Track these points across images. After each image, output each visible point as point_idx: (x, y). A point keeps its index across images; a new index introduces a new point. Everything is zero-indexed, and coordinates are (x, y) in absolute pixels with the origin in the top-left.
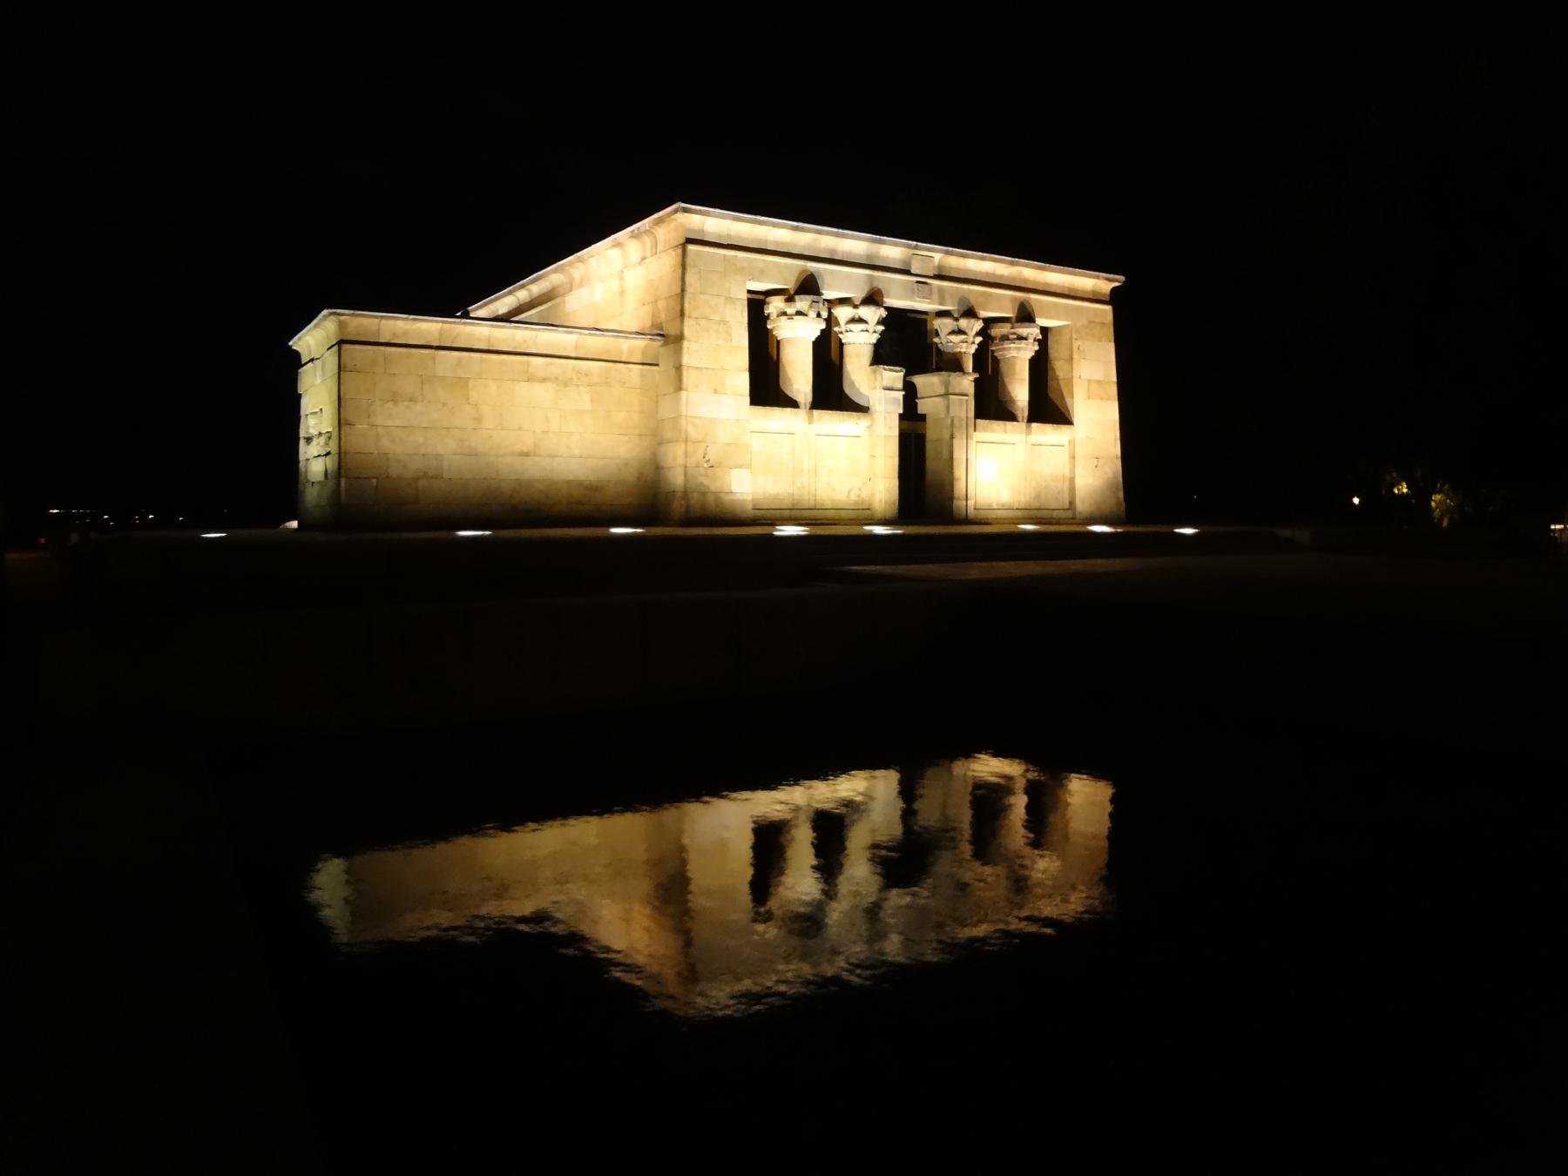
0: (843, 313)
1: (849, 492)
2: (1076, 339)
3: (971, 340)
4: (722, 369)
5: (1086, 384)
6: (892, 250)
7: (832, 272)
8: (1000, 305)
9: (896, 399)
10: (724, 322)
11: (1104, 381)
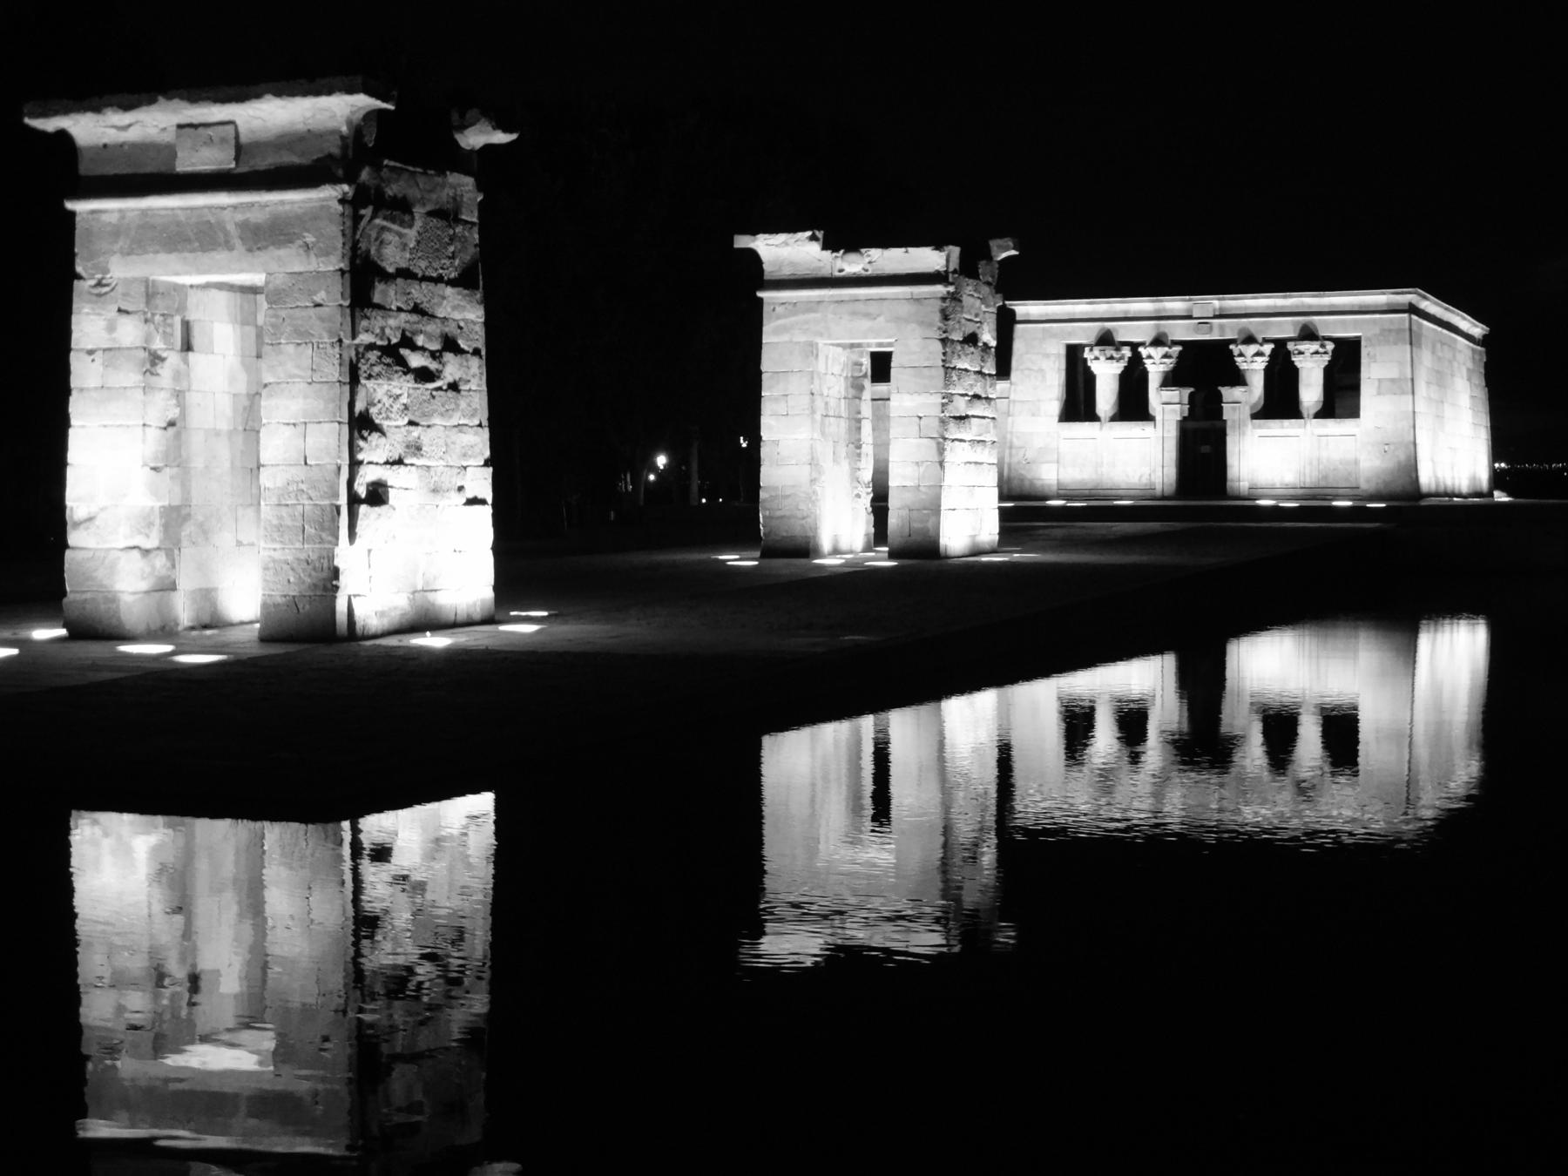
0: (1143, 351)
1: (1141, 477)
2: (1366, 347)
3: (1249, 359)
4: (1039, 401)
5: (1376, 383)
6: (1175, 304)
7: (1125, 326)
8: (1285, 328)
9: (1174, 411)
10: (1041, 370)
11: (1400, 379)
